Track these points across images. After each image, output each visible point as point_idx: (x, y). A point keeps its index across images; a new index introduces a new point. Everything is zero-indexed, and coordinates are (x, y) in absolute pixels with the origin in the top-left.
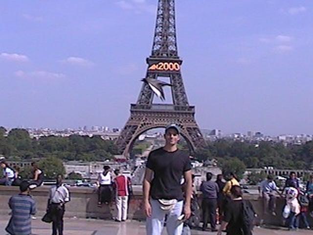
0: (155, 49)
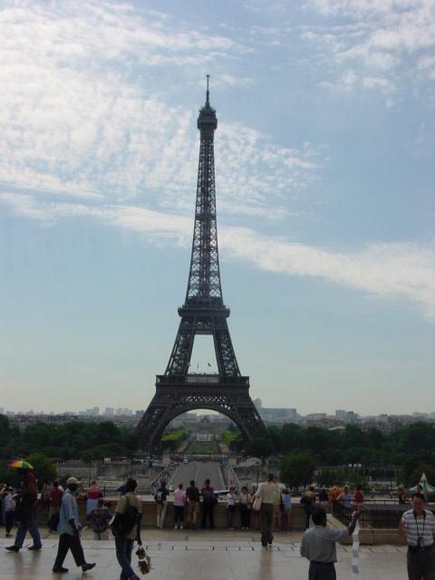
0: (190, 295)
